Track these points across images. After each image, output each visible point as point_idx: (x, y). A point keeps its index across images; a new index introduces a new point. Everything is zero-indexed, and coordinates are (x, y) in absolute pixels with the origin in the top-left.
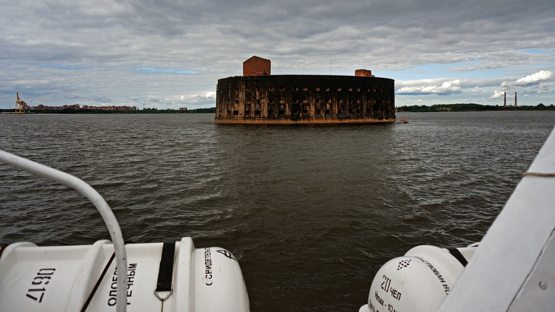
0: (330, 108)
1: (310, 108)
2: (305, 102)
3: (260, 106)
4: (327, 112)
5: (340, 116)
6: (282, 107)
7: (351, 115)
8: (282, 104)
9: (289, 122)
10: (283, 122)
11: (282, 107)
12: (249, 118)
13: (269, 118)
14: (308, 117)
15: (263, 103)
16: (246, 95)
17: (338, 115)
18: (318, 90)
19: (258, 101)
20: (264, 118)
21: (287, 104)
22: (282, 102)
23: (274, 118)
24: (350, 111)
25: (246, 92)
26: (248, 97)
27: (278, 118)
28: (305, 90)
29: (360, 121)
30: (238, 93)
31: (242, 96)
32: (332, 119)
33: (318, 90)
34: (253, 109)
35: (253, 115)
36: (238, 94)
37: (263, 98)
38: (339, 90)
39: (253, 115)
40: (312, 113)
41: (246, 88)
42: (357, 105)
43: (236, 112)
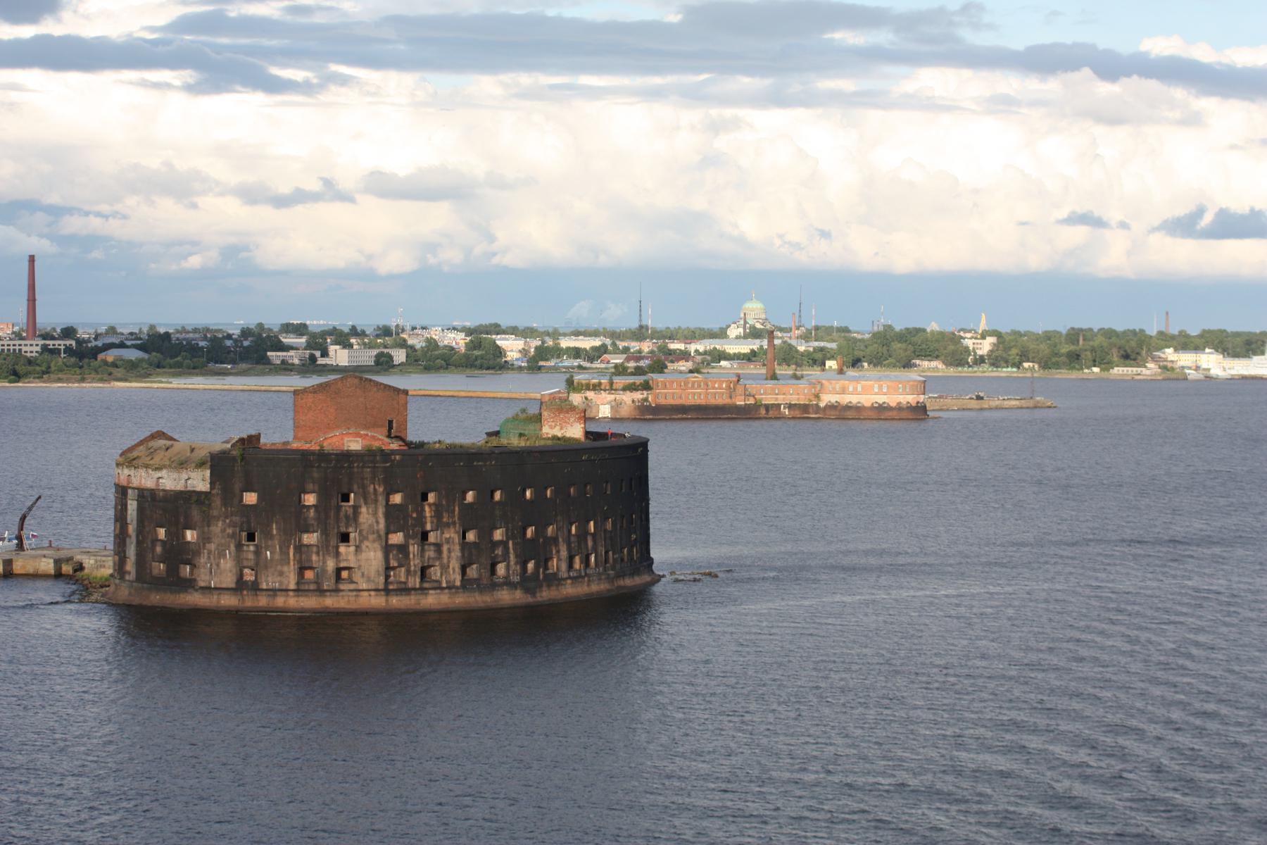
14: (553, 580)
15: (448, 541)
16: (388, 516)
22: (498, 535)
31: (370, 517)
37: (448, 525)
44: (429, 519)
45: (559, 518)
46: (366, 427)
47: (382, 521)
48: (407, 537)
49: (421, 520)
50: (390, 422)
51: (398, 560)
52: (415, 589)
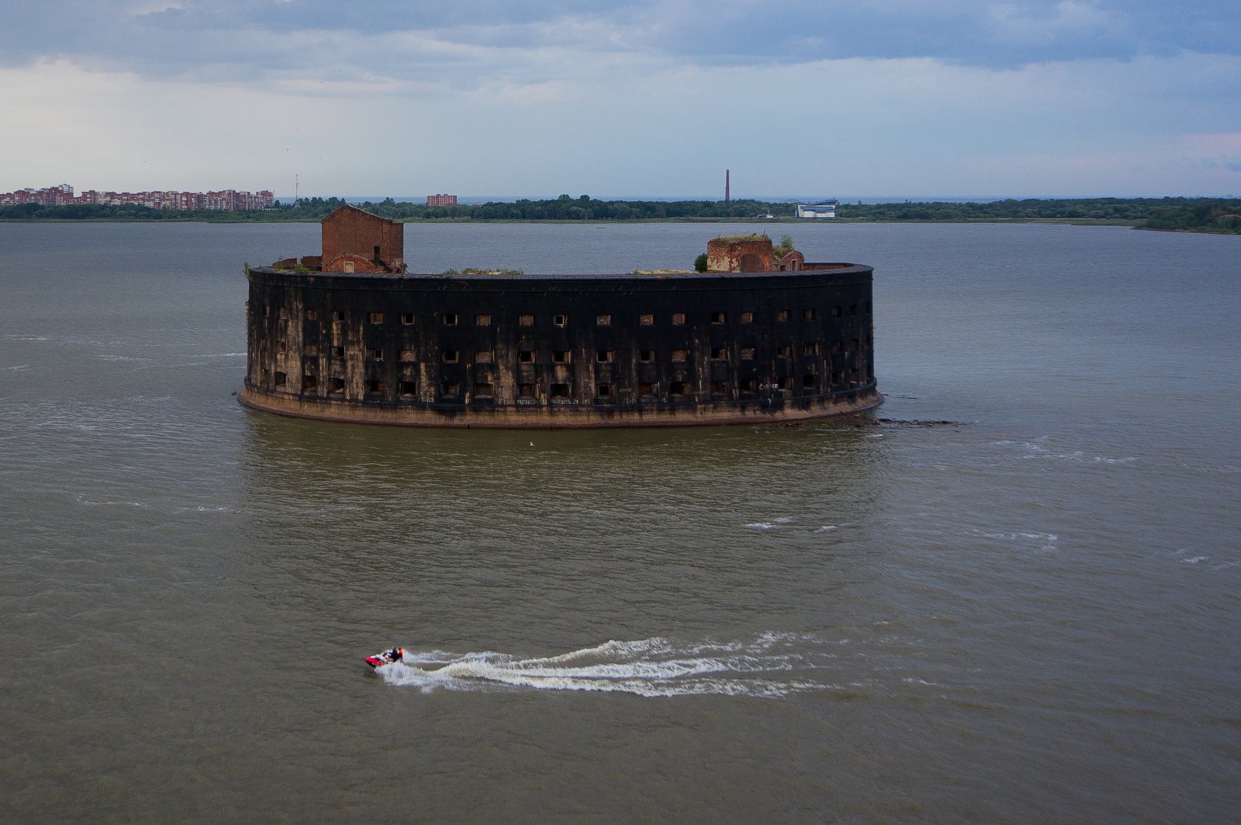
0: (568, 379)
1: (498, 378)
2: (484, 358)
3: (344, 364)
4: (558, 390)
6: (408, 372)
7: (646, 398)
8: (409, 364)
9: (429, 417)
10: (411, 417)
11: (408, 372)
12: (313, 399)
13: (368, 402)
14: (492, 406)
15: (352, 357)
16: (304, 330)
17: (596, 401)
18: (527, 321)
19: (341, 351)
20: (354, 403)
21: (422, 366)
22: (408, 356)
23: (383, 407)
24: (645, 385)
25: (306, 320)
26: (311, 334)
27: (396, 406)
28: (484, 321)
29: (683, 417)
30: (286, 321)
31: (294, 331)
32: (575, 410)
33: (527, 321)
34: (323, 374)
35: (322, 391)
36: (286, 326)
37: (353, 343)
38: (605, 321)
39: (322, 391)
40: (506, 395)
41: (305, 310)
42: (672, 368)
43: (281, 378)
44: (336, 337)
45: (500, 346)
46: (356, 253)
47: (301, 334)
48: (318, 350)
49: (329, 337)
50: (377, 249)
51: (311, 370)
52: (321, 398)
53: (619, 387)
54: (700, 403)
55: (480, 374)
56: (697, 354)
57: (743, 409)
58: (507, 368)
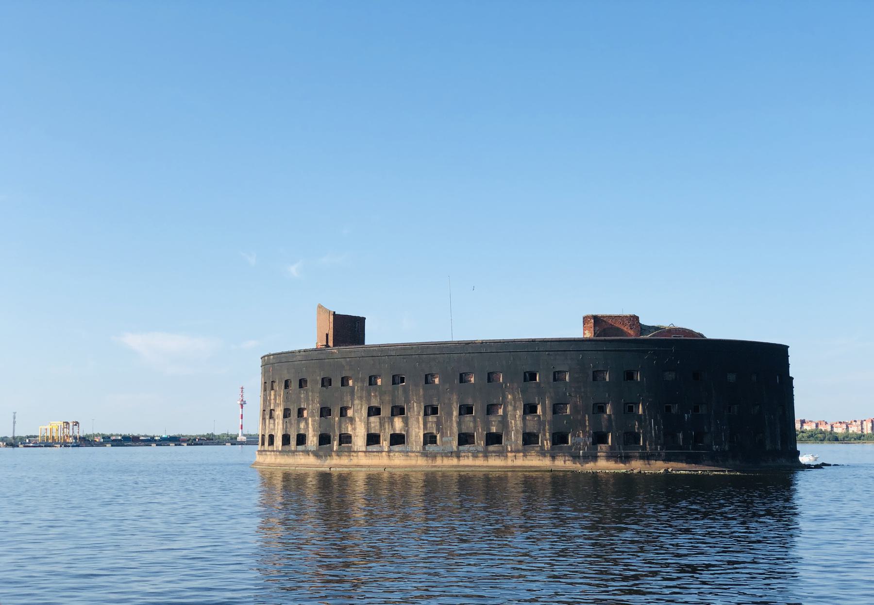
1: (354, 429)
4: (397, 439)
5: (431, 448)
6: (302, 425)
21: (310, 419)
45: (356, 402)
53: (442, 437)
54: (511, 452)
55: (343, 426)
56: (510, 408)
57: (553, 458)
58: (360, 421)
